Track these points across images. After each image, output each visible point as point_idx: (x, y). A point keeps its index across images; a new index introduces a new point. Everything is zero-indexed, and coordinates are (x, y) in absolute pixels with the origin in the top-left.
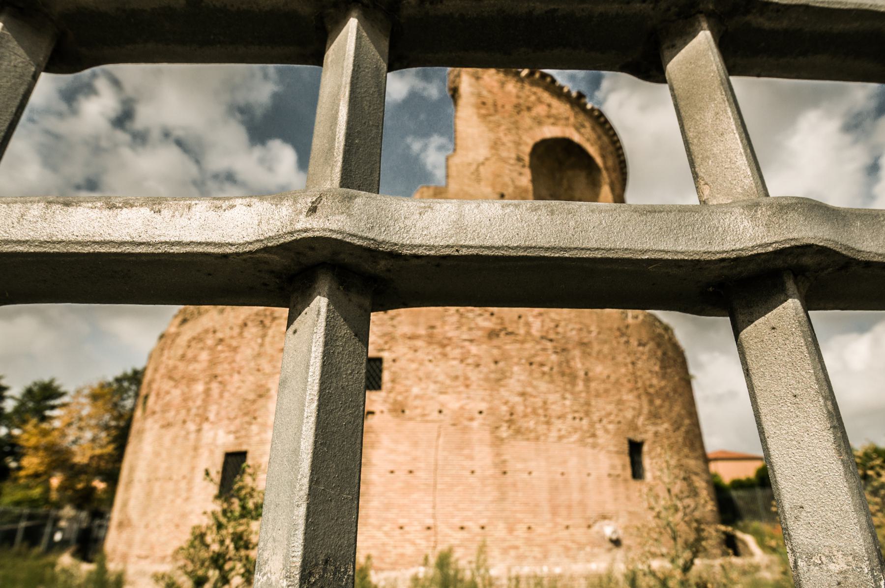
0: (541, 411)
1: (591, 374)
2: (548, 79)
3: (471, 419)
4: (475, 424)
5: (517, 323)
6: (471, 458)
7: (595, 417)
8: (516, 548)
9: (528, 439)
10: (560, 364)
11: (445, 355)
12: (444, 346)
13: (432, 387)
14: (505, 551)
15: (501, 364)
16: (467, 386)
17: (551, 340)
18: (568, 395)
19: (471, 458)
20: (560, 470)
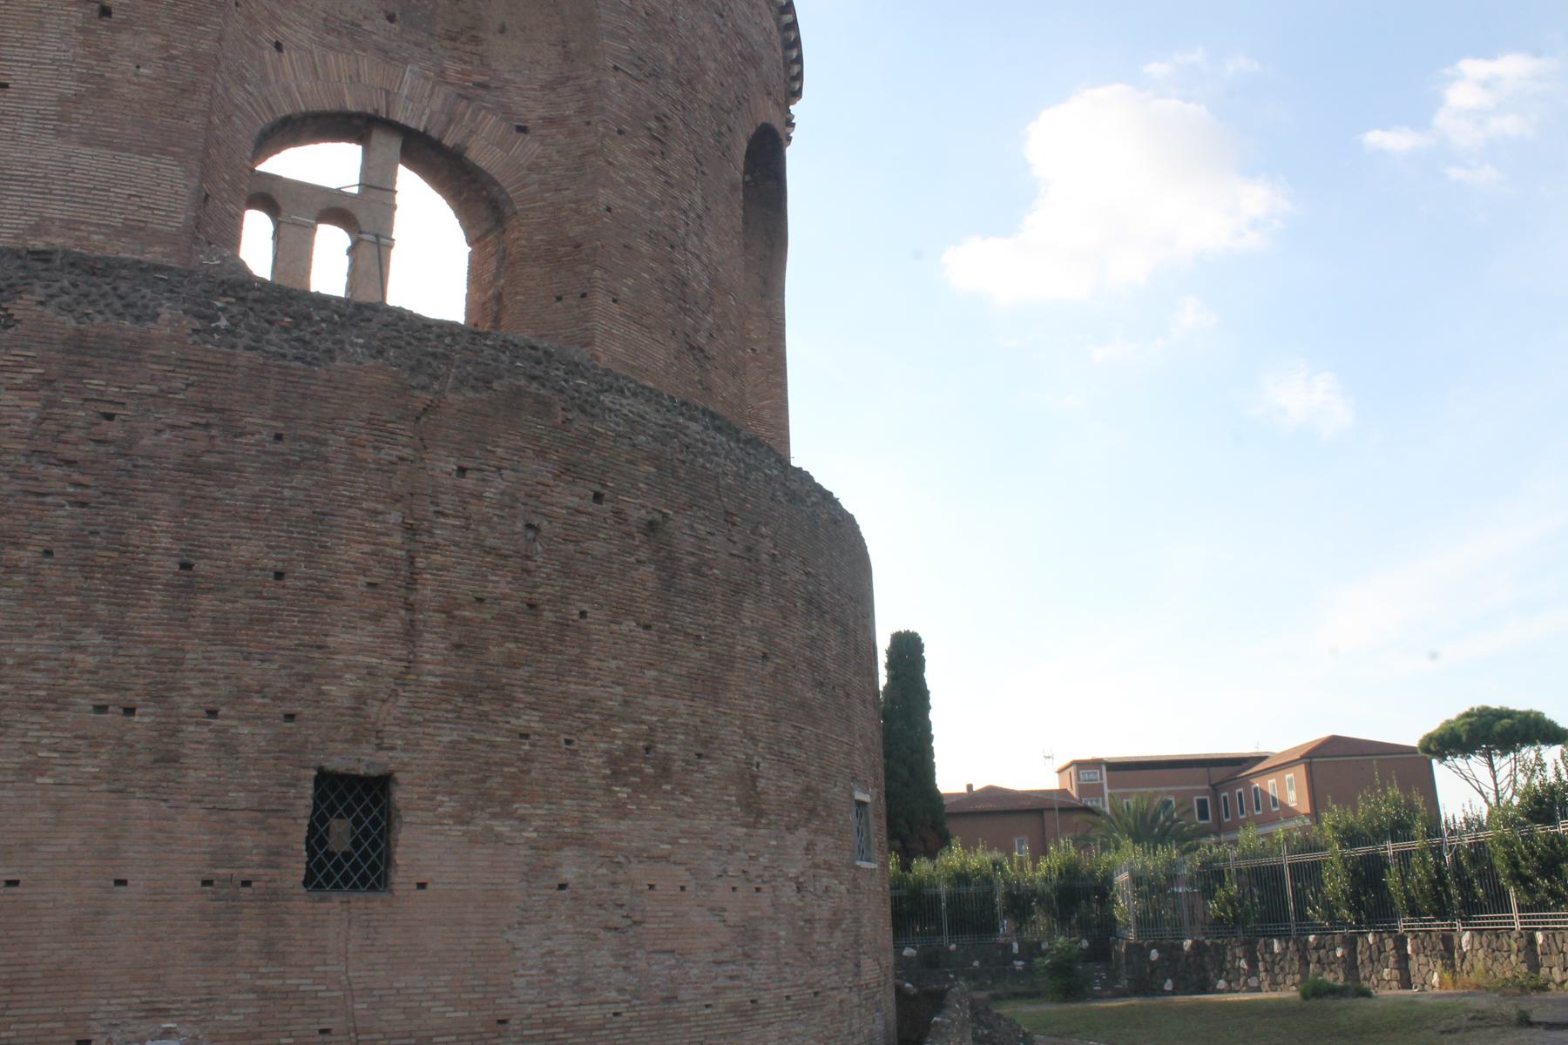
1: (202, 566)
7: (186, 704)
17: (70, 463)
18: (92, 637)
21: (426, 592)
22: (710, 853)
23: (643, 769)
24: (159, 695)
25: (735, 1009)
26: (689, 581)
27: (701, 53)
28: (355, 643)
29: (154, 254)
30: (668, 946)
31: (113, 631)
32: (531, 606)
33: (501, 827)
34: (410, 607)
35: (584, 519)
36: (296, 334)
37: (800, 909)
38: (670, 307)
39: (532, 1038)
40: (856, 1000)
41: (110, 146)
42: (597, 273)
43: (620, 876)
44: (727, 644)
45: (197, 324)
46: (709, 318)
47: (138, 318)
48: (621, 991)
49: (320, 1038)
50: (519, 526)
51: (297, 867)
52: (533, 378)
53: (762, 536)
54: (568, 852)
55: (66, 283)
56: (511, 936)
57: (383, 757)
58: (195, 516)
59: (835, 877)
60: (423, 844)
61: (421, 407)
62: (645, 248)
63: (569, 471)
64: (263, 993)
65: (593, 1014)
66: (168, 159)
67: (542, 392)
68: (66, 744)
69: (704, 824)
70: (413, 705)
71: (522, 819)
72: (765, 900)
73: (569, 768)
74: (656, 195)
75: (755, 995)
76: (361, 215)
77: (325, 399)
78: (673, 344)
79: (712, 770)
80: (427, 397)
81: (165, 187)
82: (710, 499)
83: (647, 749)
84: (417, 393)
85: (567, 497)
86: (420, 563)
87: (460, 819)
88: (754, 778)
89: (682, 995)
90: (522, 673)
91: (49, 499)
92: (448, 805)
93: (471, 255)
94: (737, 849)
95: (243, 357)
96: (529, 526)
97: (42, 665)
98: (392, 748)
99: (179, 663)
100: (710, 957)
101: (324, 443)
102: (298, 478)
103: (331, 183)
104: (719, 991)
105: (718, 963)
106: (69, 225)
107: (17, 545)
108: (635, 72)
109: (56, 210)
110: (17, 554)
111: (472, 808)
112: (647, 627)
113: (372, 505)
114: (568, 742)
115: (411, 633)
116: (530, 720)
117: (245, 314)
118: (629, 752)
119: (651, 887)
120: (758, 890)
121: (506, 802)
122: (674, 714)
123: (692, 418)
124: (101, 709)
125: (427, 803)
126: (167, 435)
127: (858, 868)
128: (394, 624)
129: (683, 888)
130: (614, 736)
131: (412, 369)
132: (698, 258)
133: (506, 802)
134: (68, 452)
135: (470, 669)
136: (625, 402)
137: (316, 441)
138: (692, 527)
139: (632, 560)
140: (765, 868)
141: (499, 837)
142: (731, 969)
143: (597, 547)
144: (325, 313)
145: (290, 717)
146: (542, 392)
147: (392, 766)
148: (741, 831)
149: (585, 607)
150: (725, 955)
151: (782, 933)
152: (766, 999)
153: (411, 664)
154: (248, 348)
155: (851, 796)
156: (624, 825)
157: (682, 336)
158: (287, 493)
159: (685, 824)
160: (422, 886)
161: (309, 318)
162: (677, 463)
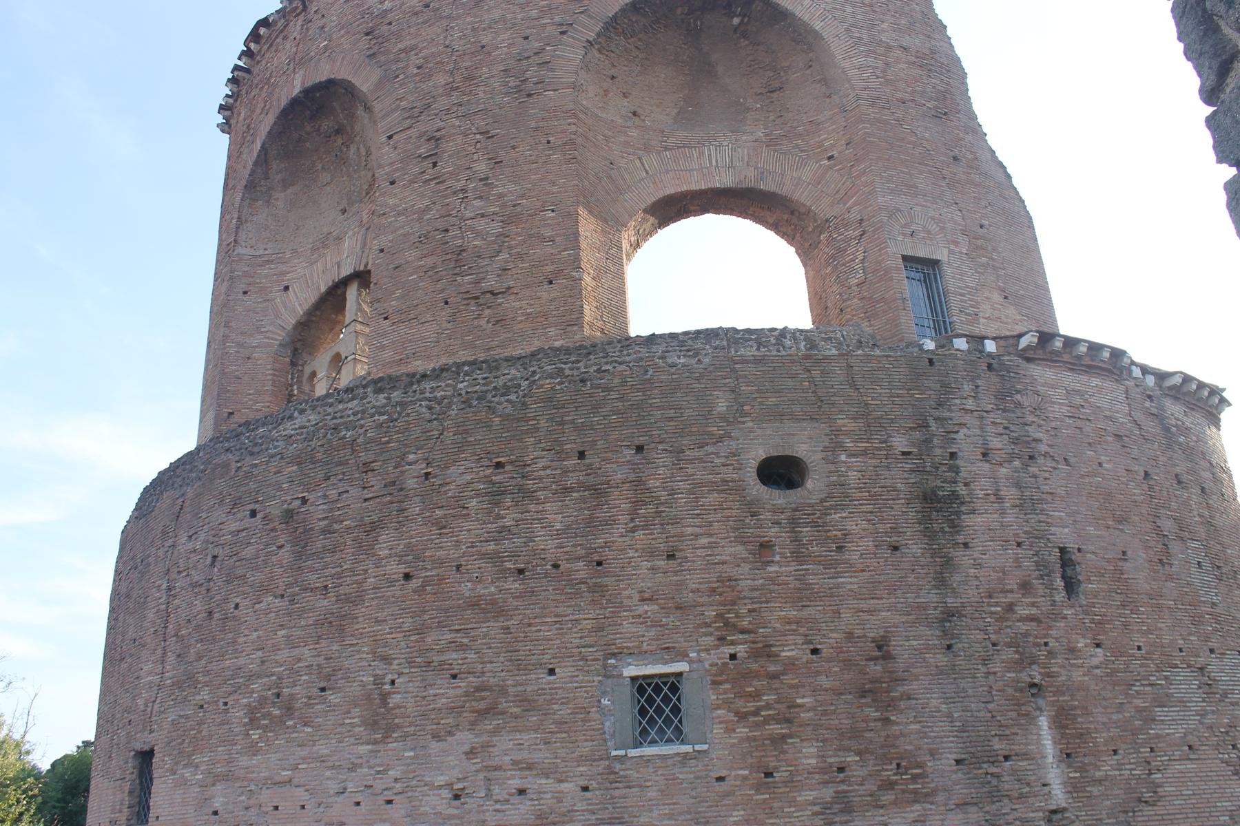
2: (262, 31)
22: (328, 773)
23: (277, 711)
26: (319, 543)
27: (485, 40)
33: (187, 774)
35: (244, 534)
37: (450, 817)
38: (440, 286)
43: (252, 802)
44: (356, 582)
46: (504, 256)
53: (410, 464)
54: (219, 786)
61: (178, 508)
62: (411, 255)
69: (323, 749)
73: (221, 724)
74: (426, 202)
78: (445, 313)
79: (334, 698)
83: (278, 695)
88: (384, 697)
90: (203, 662)
101: (149, 556)
108: (406, 123)
111: (176, 763)
112: (282, 596)
114: (226, 704)
116: (204, 695)
118: (263, 701)
119: (276, 808)
120: (389, 802)
122: (300, 660)
129: (303, 807)
132: (483, 216)
140: (396, 780)
143: (249, 552)
148: (364, 749)
149: (238, 600)
155: (609, 674)
159: (304, 752)
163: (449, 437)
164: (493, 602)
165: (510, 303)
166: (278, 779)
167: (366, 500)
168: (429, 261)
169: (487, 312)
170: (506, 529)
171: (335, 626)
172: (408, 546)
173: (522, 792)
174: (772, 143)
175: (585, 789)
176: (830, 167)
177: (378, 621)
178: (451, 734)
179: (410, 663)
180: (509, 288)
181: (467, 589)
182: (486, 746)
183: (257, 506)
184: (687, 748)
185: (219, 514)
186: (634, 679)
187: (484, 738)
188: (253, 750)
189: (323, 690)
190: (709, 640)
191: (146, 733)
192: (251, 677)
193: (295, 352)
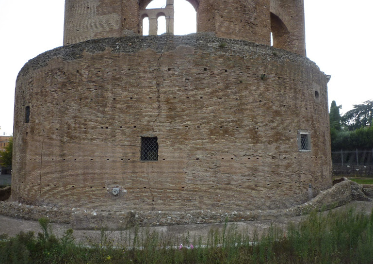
0: (83, 126)
1: (117, 99)
3: (53, 133)
4: (54, 136)
5: (76, 75)
6: (52, 152)
7: (116, 126)
8: (67, 196)
9: (75, 142)
10: (96, 96)
11: (46, 101)
12: (45, 96)
13: (42, 118)
14: (62, 197)
15: (66, 101)
16: (52, 116)
17: (94, 82)
18: (100, 115)
19: (52, 152)
20: (90, 158)
21: (162, 98)
22: (240, 150)
24: (111, 125)
25: (249, 187)
28: (149, 110)
29: (116, 35)
30: (228, 172)
31: (103, 113)
32: (188, 98)
34: (159, 101)
35: (202, 75)
36: (132, 46)
38: (240, 14)
39: (190, 191)
40: (298, 185)
41: (105, 14)
42: (216, 11)
45: (112, 49)
47: (102, 50)
48: (213, 182)
49: (144, 189)
50: (184, 79)
51: (138, 156)
52: (187, 44)
53: (260, 70)
54: (198, 152)
55: (91, 46)
56: (184, 170)
57: (154, 133)
58: (115, 89)
59: (289, 154)
60: (164, 151)
61: (159, 57)
63: (197, 64)
64: (133, 180)
65: (207, 187)
66: (115, 13)
67: (189, 47)
68: (97, 135)
69: (238, 144)
70: (160, 122)
71: (187, 145)
72: (260, 161)
75: (256, 184)
76: (165, 13)
77: (138, 59)
79: (241, 130)
80: (160, 54)
81: (114, 20)
82: (241, 64)
84: (158, 54)
85: (195, 70)
86: (160, 91)
87: (172, 145)
88: (256, 132)
89: (232, 183)
90: (186, 112)
91: (91, 89)
92: (169, 142)
93: (197, 14)
94: (250, 149)
95: (121, 53)
96: (186, 79)
97: (93, 121)
98: (156, 131)
99: (114, 118)
100: (241, 175)
102: (134, 77)
103: (159, 7)
104: (244, 182)
105: (245, 176)
106: (100, 33)
107: (88, 99)
109: (98, 31)
110: (87, 100)
111: (175, 143)
112: (221, 98)
113: (149, 81)
115: (159, 107)
116: (189, 123)
117: (122, 44)
118: (215, 129)
119: (223, 159)
120: (257, 159)
121: (182, 141)
122: (229, 118)
123: (236, 44)
124: (102, 128)
125: (164, 143)
126: (109, 73)
127: (300, 152)
128: (156, 105)
130: (211, 125)
131: (157, 48)
133: (182, 141)
134: (93, 80)
135: (173, 113)
136: (214, 44)
137: (137, 69)
138: (234, 72)
139: (216, 83)
141: (181, 149)
142: (247, 177)
144: (138, 40)
145: (135, 127)
146: (189, 47)
147: (156, 135)
148: (251, 145)
150: (246, 174)
151: (266, 169)
152: (260, 184)
153: (159, 113)
154: (122, 52)
155: (299, 134)
156: (214, 145)
157: (245, 21)
158: (132, 81)
160: (164, 159)
161: (135, 42)
162: (229, 56)
163: (269, 67)
164: (280, 112)
165: (258, 30)
166: (223, 151)
167: (248, 77)
168: (236, 5)
169: (251, 29)
170: (281, 94)
171: (241, 110)
172: (260, 93)
173: (285, 158)
174: (282, 6)
175: (295, 158)
176: (292, 19)
177: (253, 112)
178: (272, 143)
179: (262, 124)
180: (257, 24)
181: (275, 108)
182: (279, 147)
183: (207, 67)
184: (308, 151)
185: (190, 66)
186: (301, 135)
187: (279, 145)
188: (213, 142)
189: (237, 128)
190: (310, 128)
191: (151, 132)
192: (209, 121)
193: (139, 5)
